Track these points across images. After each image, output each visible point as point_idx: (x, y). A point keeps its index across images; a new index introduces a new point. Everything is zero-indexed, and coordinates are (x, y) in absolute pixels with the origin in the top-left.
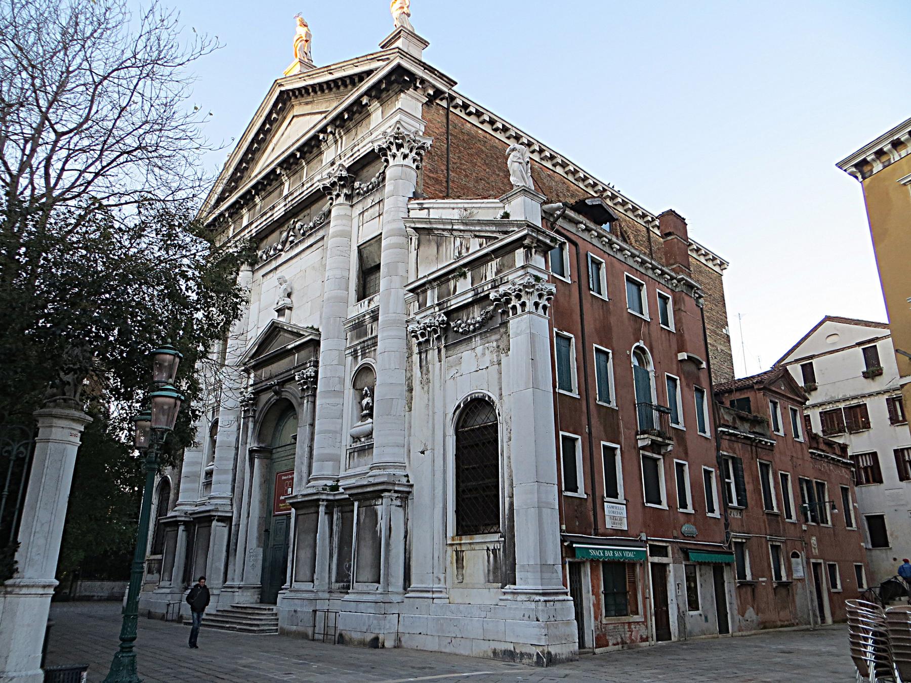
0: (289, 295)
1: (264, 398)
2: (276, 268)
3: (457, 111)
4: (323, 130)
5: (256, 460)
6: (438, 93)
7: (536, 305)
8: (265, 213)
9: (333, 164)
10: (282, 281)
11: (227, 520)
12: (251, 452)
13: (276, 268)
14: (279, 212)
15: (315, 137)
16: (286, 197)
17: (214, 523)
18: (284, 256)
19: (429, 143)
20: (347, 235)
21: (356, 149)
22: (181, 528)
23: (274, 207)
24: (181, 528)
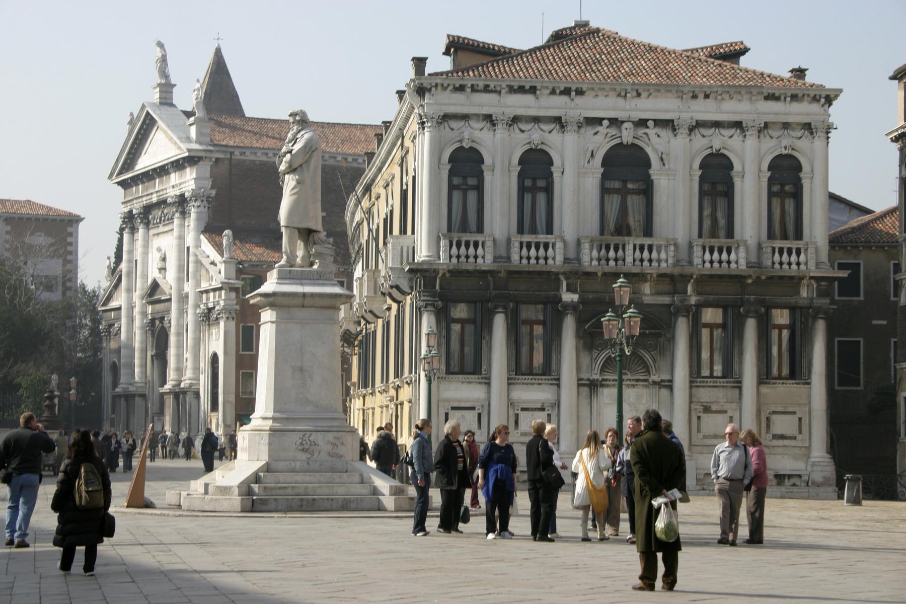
0: (164, 259)
1: (157, 322)
2: (158, 234)
3: (240, 157)
4: (167, 164)
5: (155, 362)
6: (217, 159)
7: (228, 318)
8: (148, 195)
9: (173, 187)
10: (159, 250)
11: (143, 396)
12: (152, 356)
13: (158, 234)
14: (155, 199)
15: (163, 166)
16: (157, 192)
17: (137, 398)
18: (162, 229)
19: (213, 193)
20: (181, 238)
21: (182, 186)
22: (123, 399)
23: (152, 194)
24: (123, 399)
